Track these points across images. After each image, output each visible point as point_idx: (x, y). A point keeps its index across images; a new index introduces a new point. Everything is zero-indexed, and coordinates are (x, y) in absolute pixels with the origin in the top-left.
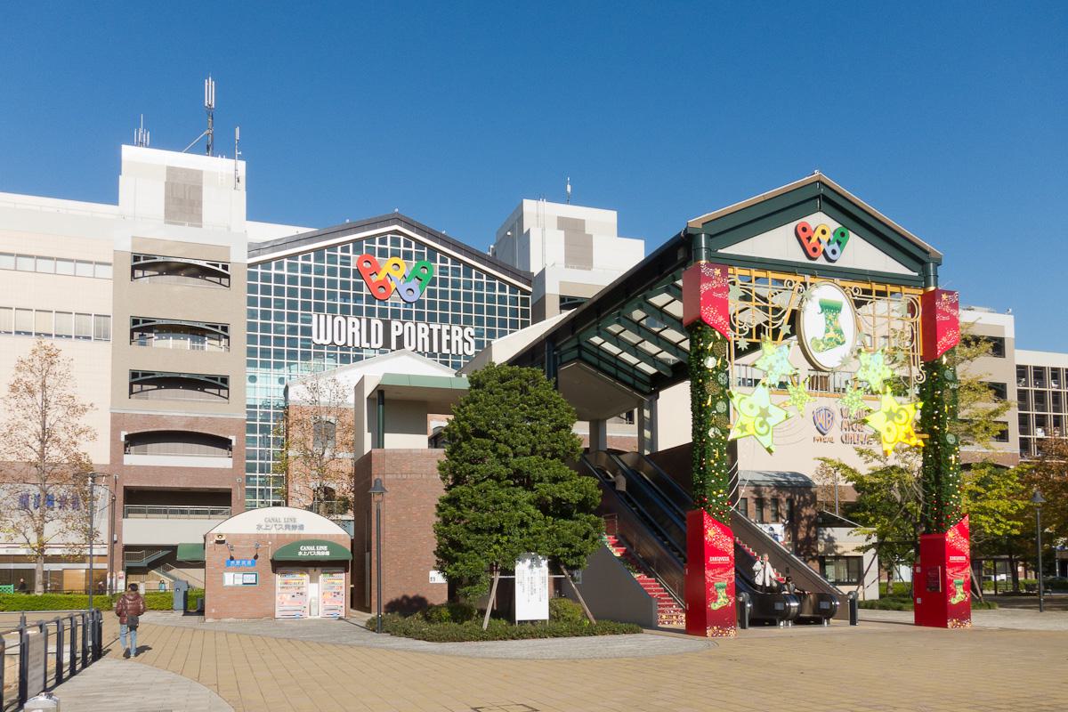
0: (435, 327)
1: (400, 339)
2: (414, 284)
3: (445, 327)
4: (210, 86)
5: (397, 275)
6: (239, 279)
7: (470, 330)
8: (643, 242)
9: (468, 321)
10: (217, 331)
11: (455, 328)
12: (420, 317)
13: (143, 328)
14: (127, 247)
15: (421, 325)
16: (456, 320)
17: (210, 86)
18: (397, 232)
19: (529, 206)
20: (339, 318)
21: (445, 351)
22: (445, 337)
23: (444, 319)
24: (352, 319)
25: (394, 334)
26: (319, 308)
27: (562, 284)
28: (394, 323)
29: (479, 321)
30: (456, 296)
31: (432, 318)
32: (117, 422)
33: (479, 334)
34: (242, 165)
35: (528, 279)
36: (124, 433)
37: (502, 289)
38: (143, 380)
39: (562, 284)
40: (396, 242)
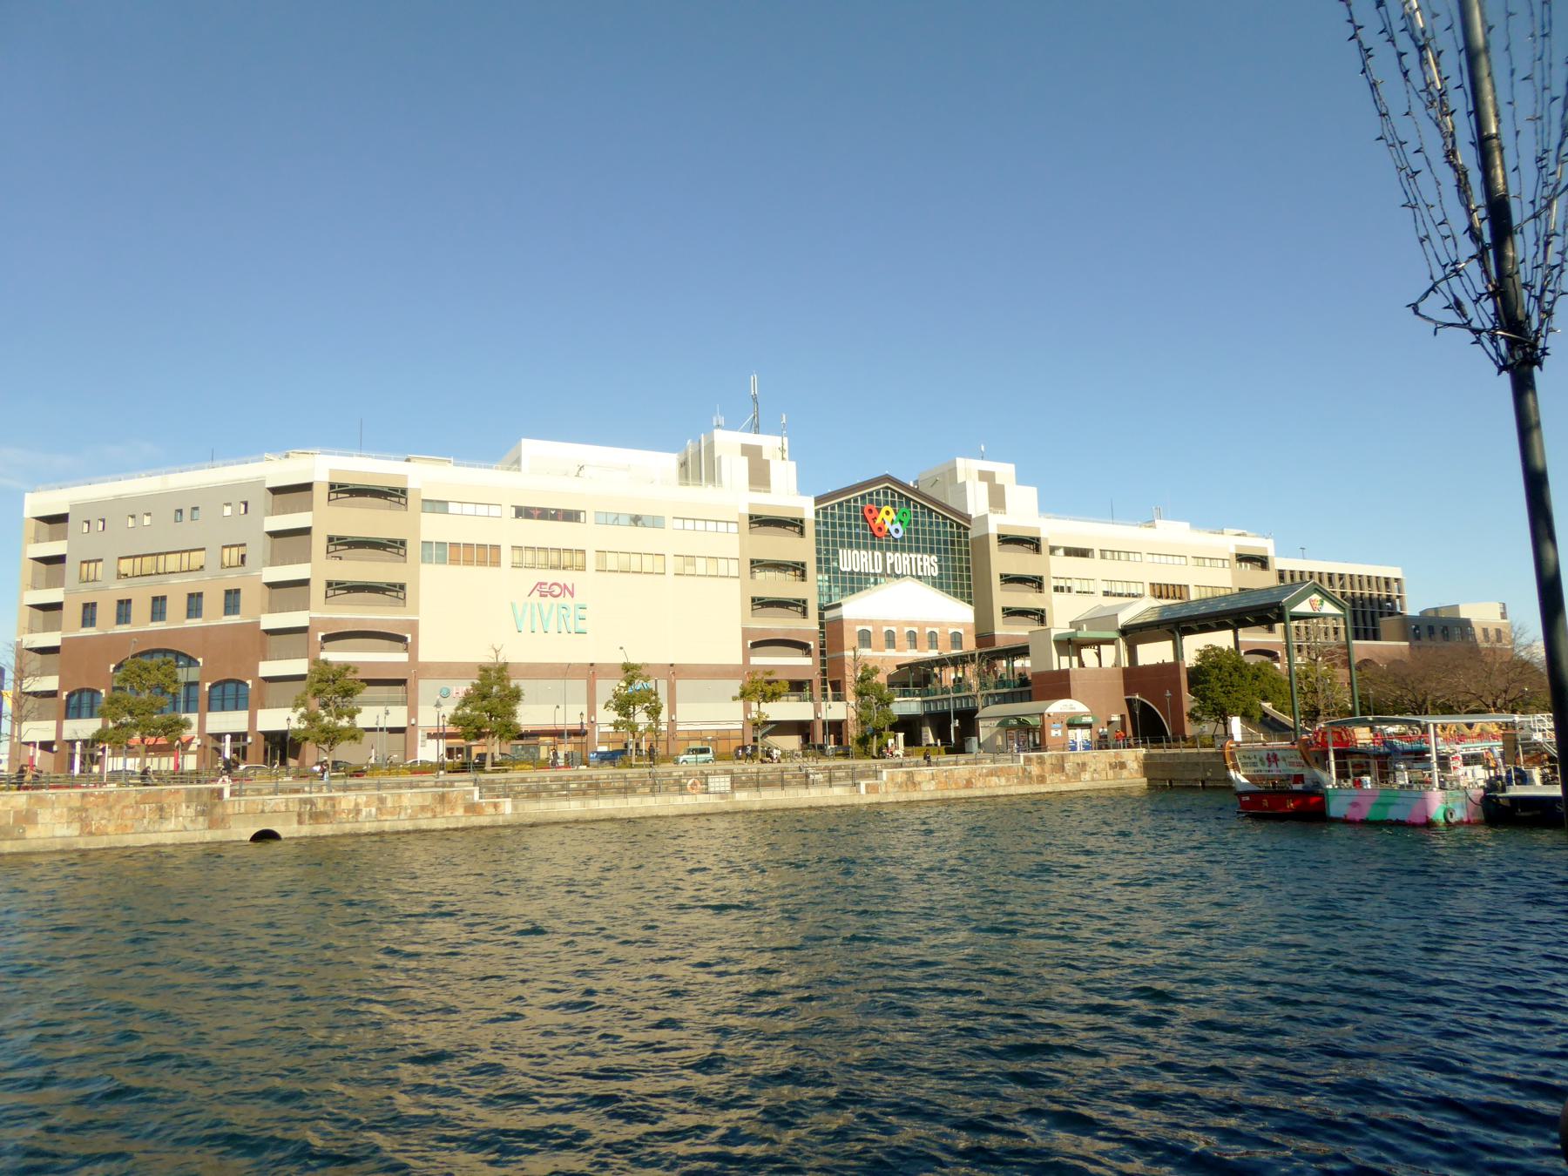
0: (913, 556)
1: (892, 565)
2: (897, 525)
3: (919, 556)
4: (754, 378)
5: (888, 519)
6: (810, 529)
7: (934, 557)
8: (1034, 490)
9: (932, 552)
10: (799, 569)
11: (925, 556)
12: (903, 550)
13: (757, 564)
14: (746, 511)
15: (905, 555)
16: (925, 551)
17: (754, 378)
18: (887, 488)
19: (961, 463)
20: (855, 552)
21: (920, 573)
22: (919, 563)
23: (918, 551)
24: (863, 552)
25: (889, 562)
26: (842, 545)
27: (999, 526)
28: (889, 554)
29: (939, 551)
30: (924, 532)
31: (910, 550)
32: (746, 633)
33: (939, 561)
34: (786, 440)
35: (968, 519)
36: (750, 642)
37: (952, 526)
38: (761, 603)
39: (999, 526)
40: (886, 494)
